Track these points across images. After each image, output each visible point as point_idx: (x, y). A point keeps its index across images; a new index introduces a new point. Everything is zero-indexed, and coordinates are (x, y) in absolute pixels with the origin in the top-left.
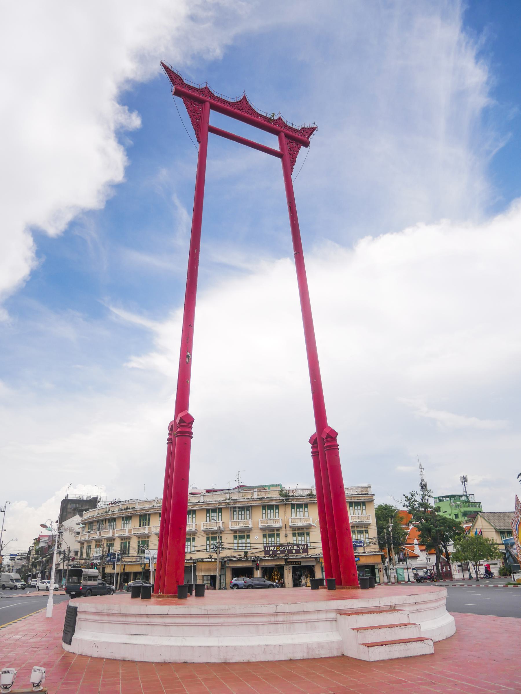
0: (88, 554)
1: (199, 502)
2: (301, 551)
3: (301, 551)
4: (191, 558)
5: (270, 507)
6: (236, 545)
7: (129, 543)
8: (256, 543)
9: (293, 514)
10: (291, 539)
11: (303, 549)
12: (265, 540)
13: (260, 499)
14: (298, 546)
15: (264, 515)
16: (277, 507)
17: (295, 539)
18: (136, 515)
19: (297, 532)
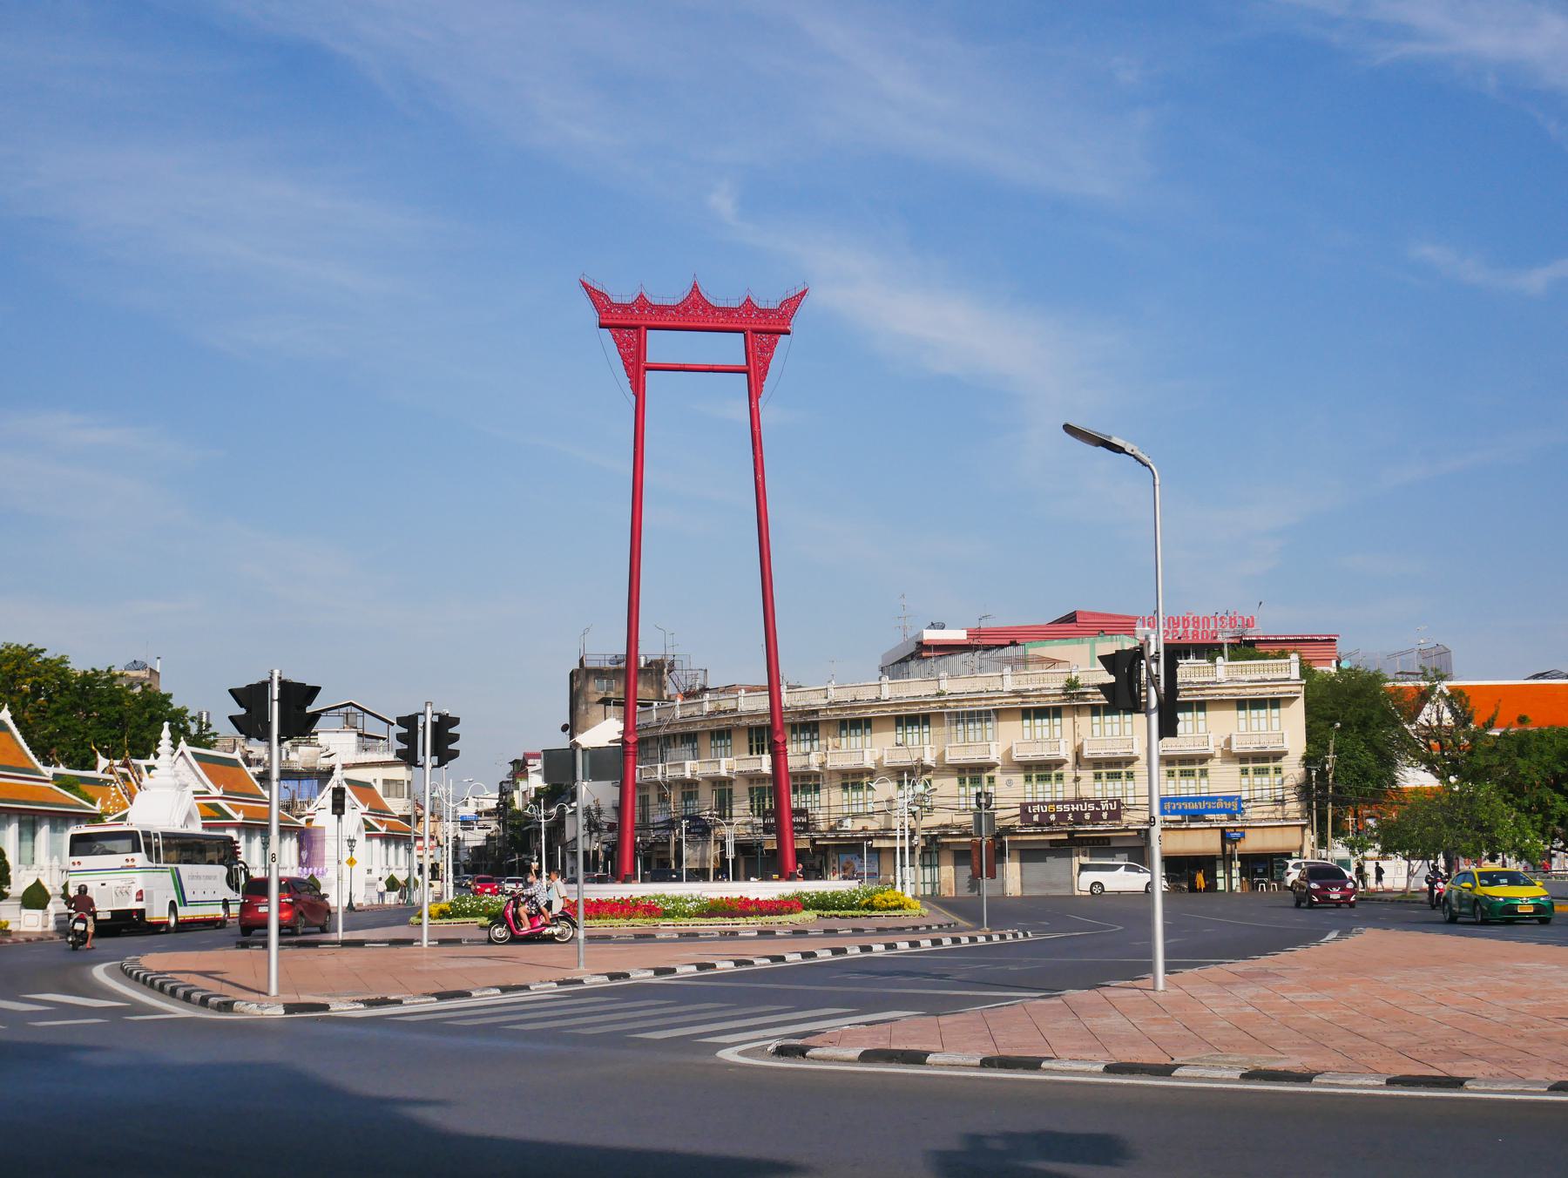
0: (644, 816)
1: (878, 699)
2: (1105, 815)
3: (1105, 815)
4: (864, 829)
5: (1042, 713)
6: (962, 800)
7: (730, 791)
8: (1010, 793)
9: (1096, 728)
10: (1091, 787)
11: (1109, 811)
12: (1029, 787)
13: (1017, 693)
14: (1097, 803)
15: (1027, 731)
16: (1057, 712)
17: (1098, 785)
18: (739, 728)
19: (1104, 771)
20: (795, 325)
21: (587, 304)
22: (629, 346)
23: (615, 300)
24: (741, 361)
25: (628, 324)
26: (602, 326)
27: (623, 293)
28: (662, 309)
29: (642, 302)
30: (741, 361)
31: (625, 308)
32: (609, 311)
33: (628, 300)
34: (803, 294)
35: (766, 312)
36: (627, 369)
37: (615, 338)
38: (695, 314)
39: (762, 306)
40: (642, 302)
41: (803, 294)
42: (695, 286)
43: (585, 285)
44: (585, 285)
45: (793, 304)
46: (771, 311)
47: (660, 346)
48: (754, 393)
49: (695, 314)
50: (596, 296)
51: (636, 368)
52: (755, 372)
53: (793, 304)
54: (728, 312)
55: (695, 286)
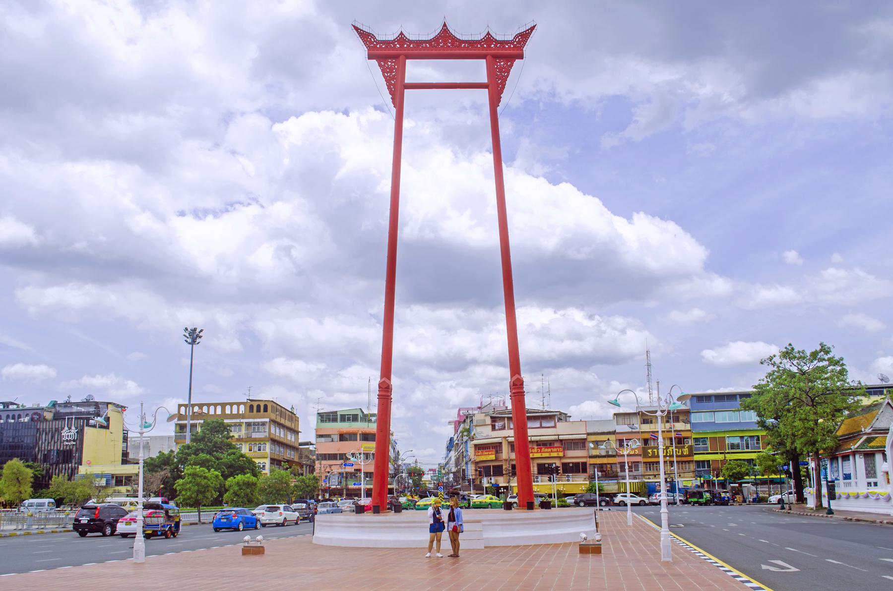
20: (527, 49)
21: (359, 42)
22: (391, 72)
23: (379, 38)
24: (484, 79)
25: (390, 55)
26: (370, 57)
27: (386, 33)
28: (418, 43)
29: (402, 39)
30: (484, 79)
31: (387, 43)
32: (375, 46)
33: (391, 38)
34: (532, 28)
35: (503, 43)
36: (389, 88)
37: (380, 65)
38: (445, 46)
39: (499, 38)
40: (402, 39)
41: (532, 28)
42: (445, 25)
43: (356, 29)
44: (356, 29)
45: (524, 36)
46: (507, 42)
47: (416, 70)
48: (495, 101)
49: (445, 46)
50: (365, 36)
51: (397, 88)
52: (495, 87)
53: (524, 36)
54: (472, 43)
55: (445, 25)
